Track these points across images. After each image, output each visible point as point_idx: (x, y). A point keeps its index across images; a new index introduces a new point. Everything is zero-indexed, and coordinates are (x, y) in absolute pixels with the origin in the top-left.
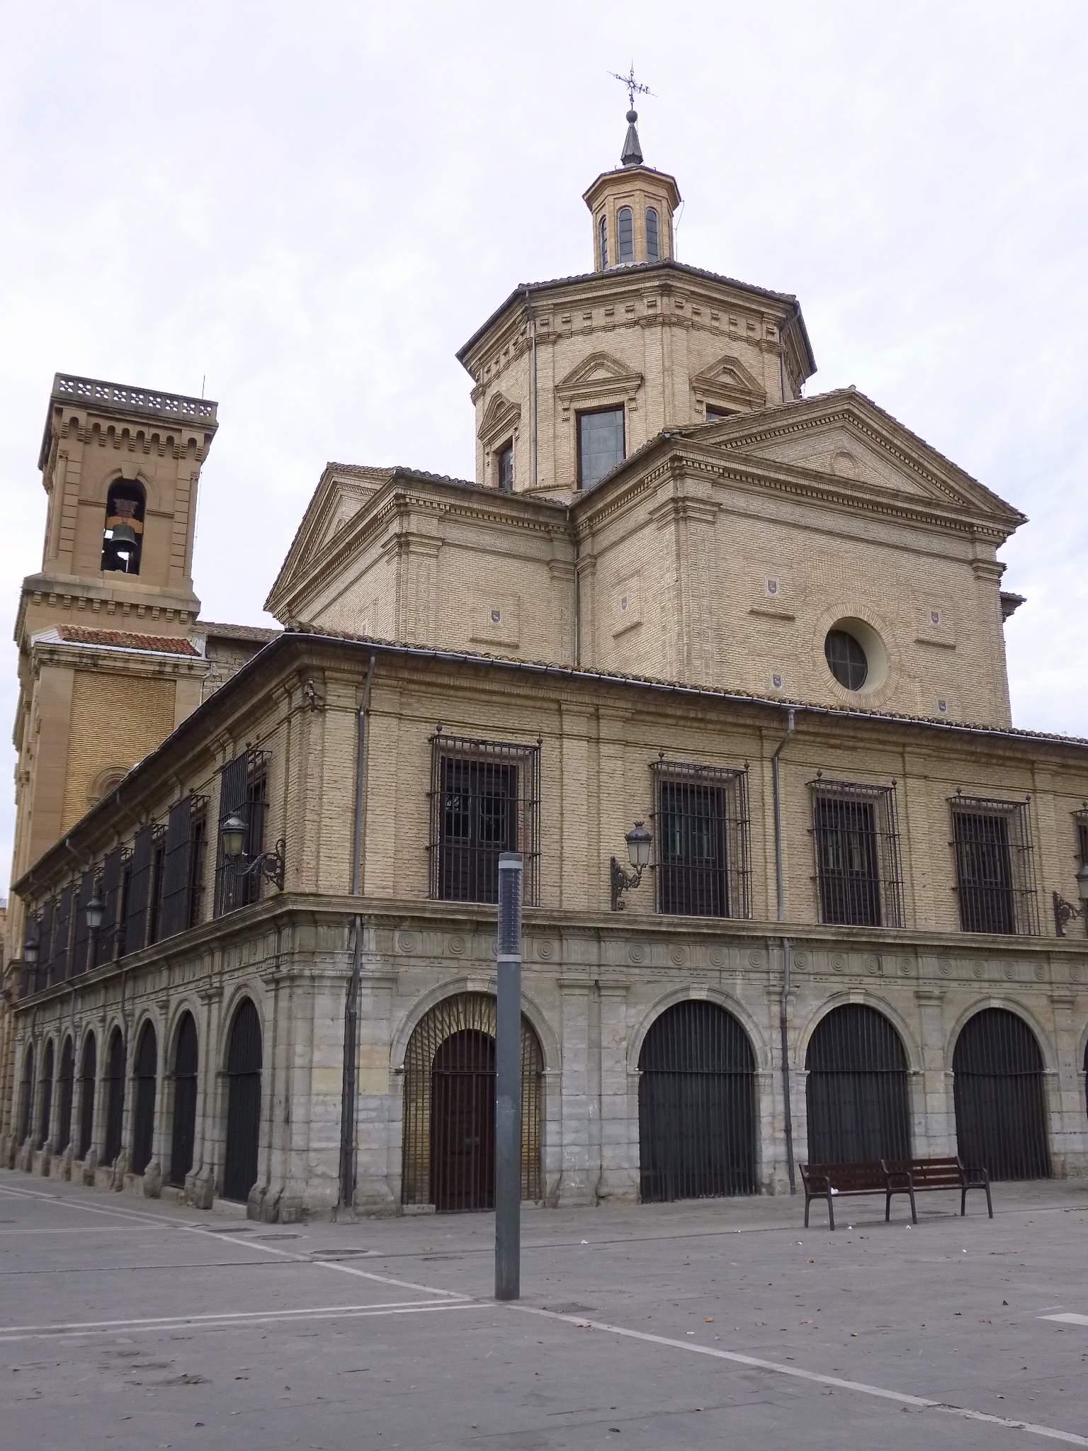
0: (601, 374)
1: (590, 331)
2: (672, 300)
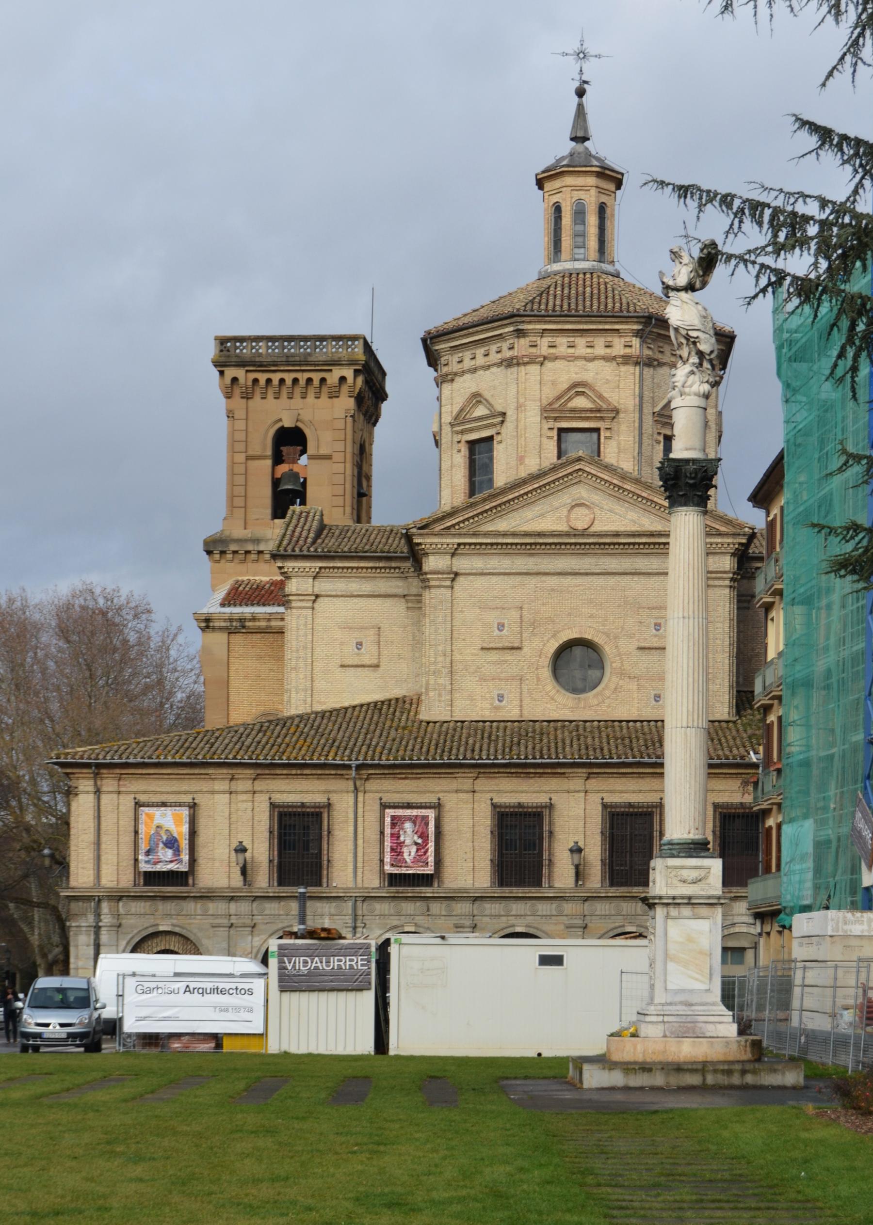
1: (474, 370)
2: (528, 339)
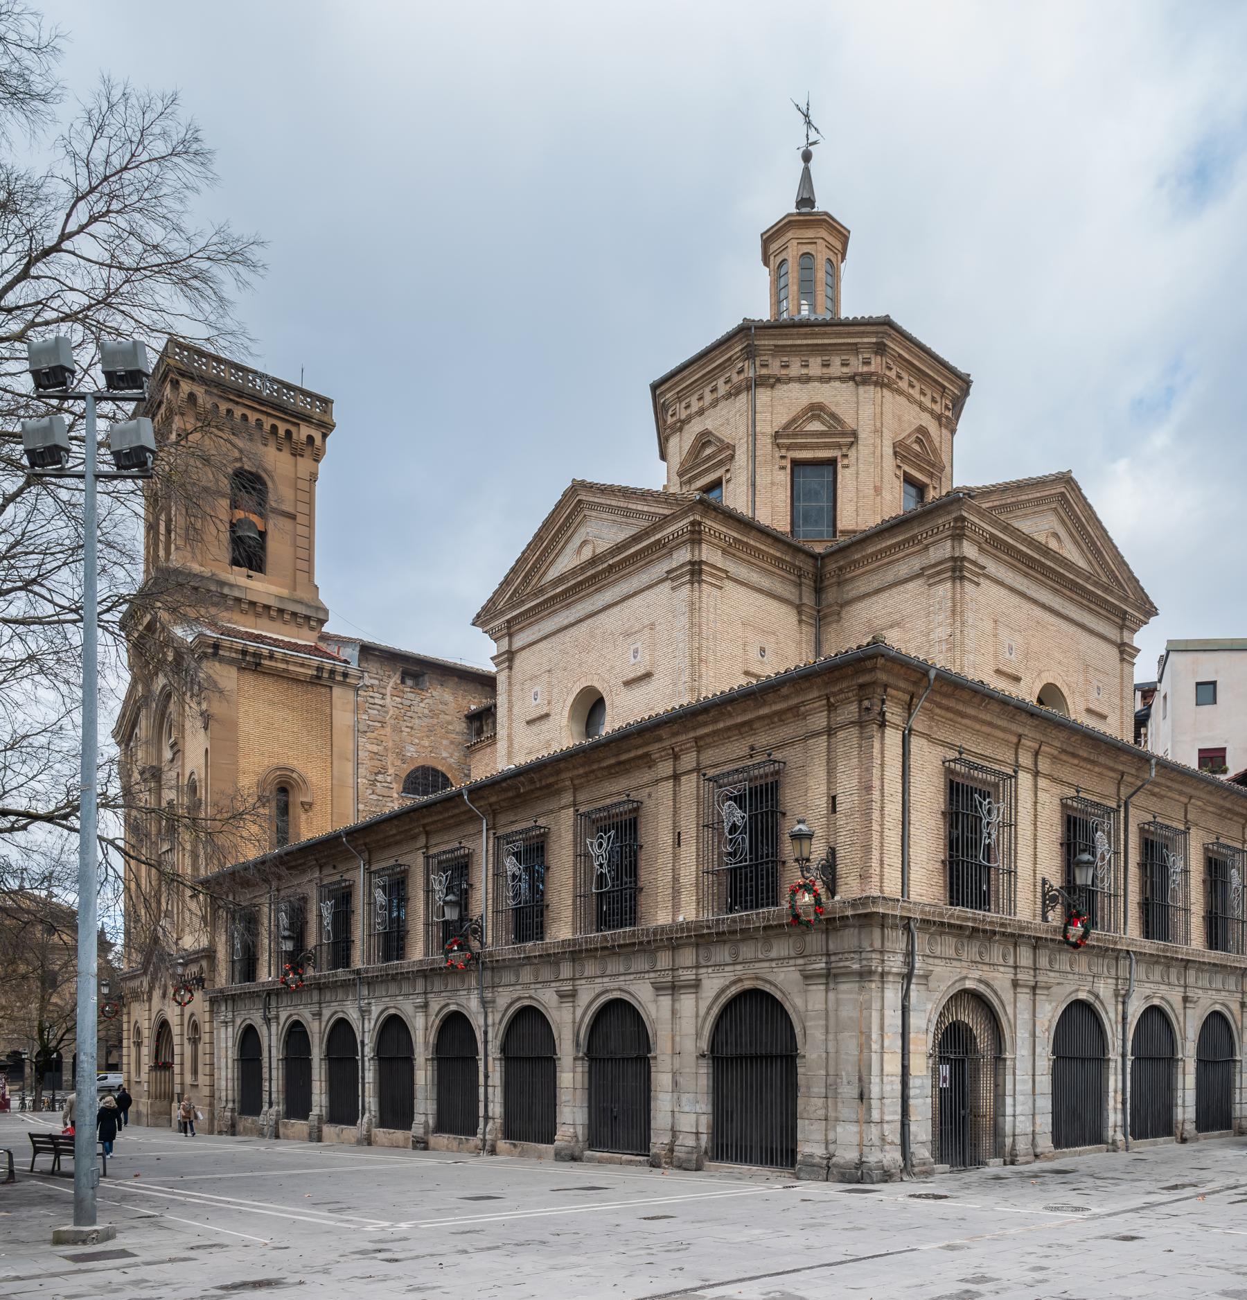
0: (816, 426)
